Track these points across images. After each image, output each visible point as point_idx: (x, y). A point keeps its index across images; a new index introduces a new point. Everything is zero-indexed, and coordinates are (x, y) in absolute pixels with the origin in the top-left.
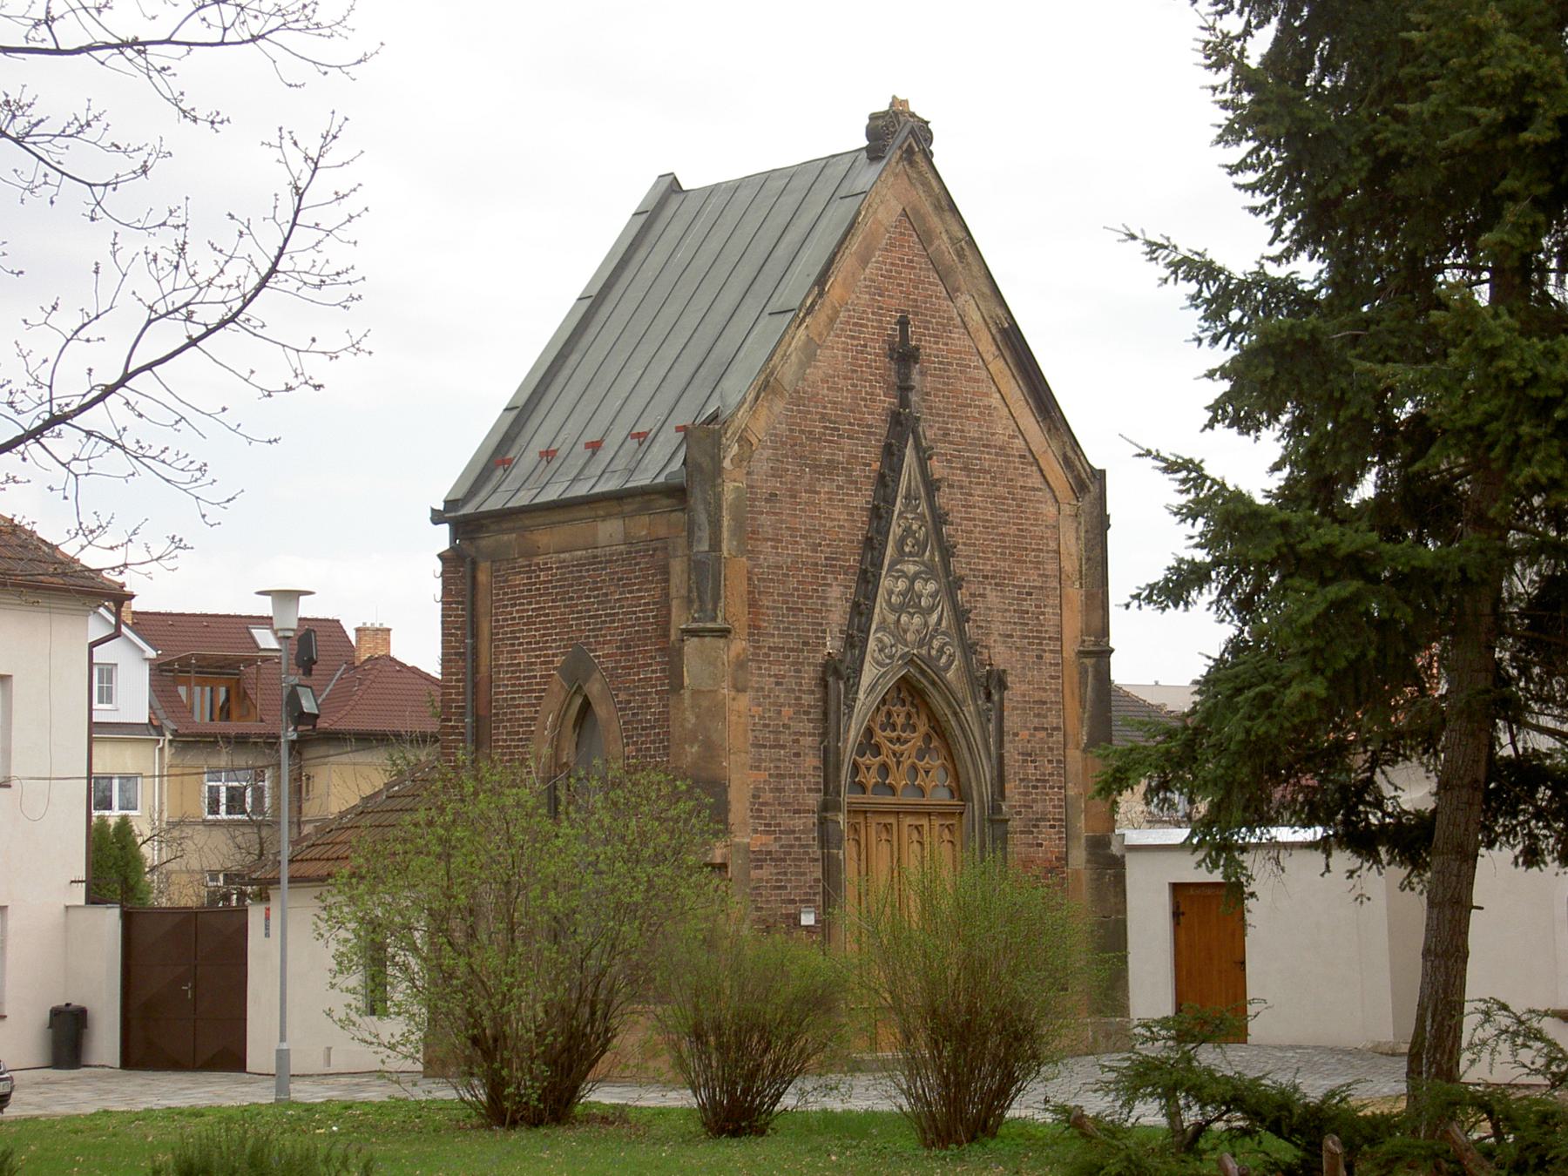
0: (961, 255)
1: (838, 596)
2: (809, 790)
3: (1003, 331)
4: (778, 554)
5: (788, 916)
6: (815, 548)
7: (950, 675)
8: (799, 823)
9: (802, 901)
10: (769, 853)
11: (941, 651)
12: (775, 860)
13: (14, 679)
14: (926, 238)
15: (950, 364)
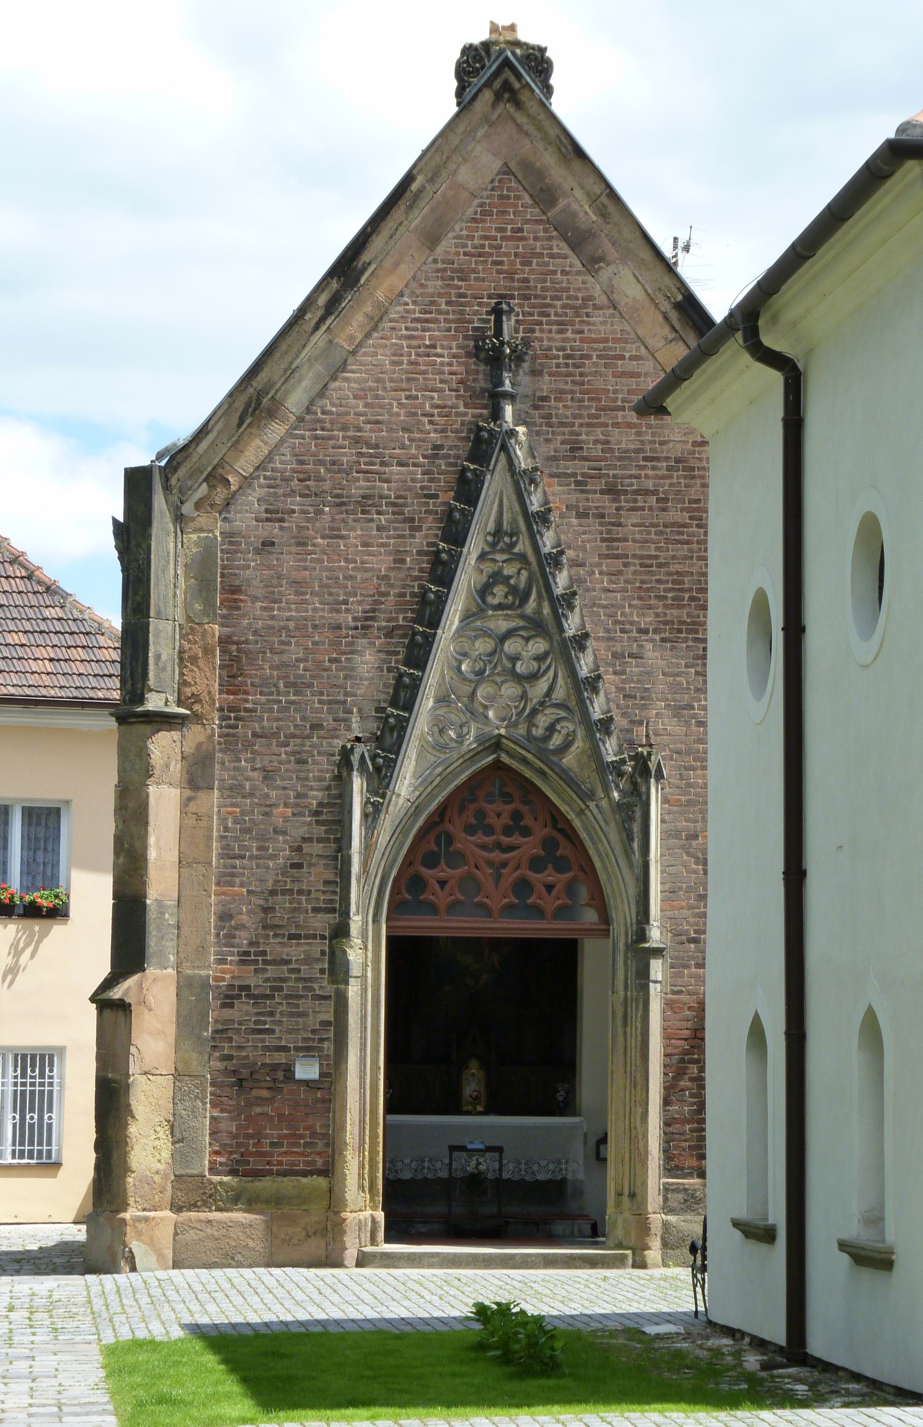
0: (603, 214)
1: (368, 663)
2: (316, 910)
3: (678, 306)
4: (273, 618)
5: (274, 1067)
6: (336, 606)
7: (569, 760)
8: (295, 951)
9: (297, 1049)
10: (247, 988)
11: (551, 729)
12: (255, 997)
13: (74, 805)
14: (545, 196)
15: (588, 357)
